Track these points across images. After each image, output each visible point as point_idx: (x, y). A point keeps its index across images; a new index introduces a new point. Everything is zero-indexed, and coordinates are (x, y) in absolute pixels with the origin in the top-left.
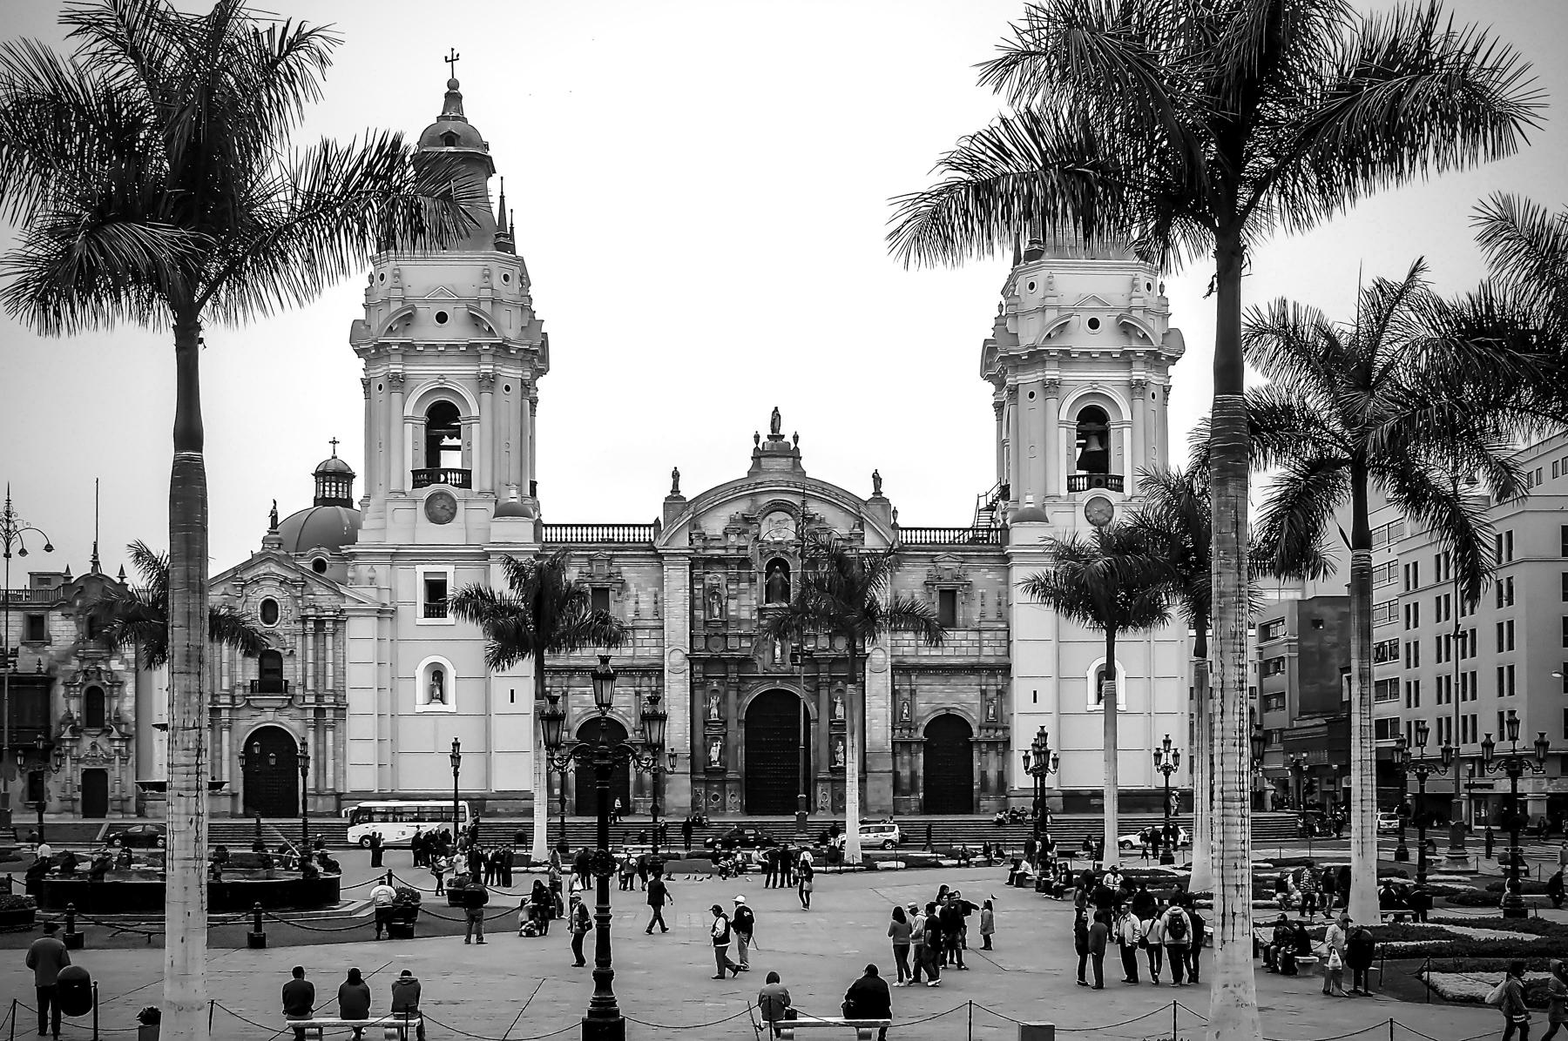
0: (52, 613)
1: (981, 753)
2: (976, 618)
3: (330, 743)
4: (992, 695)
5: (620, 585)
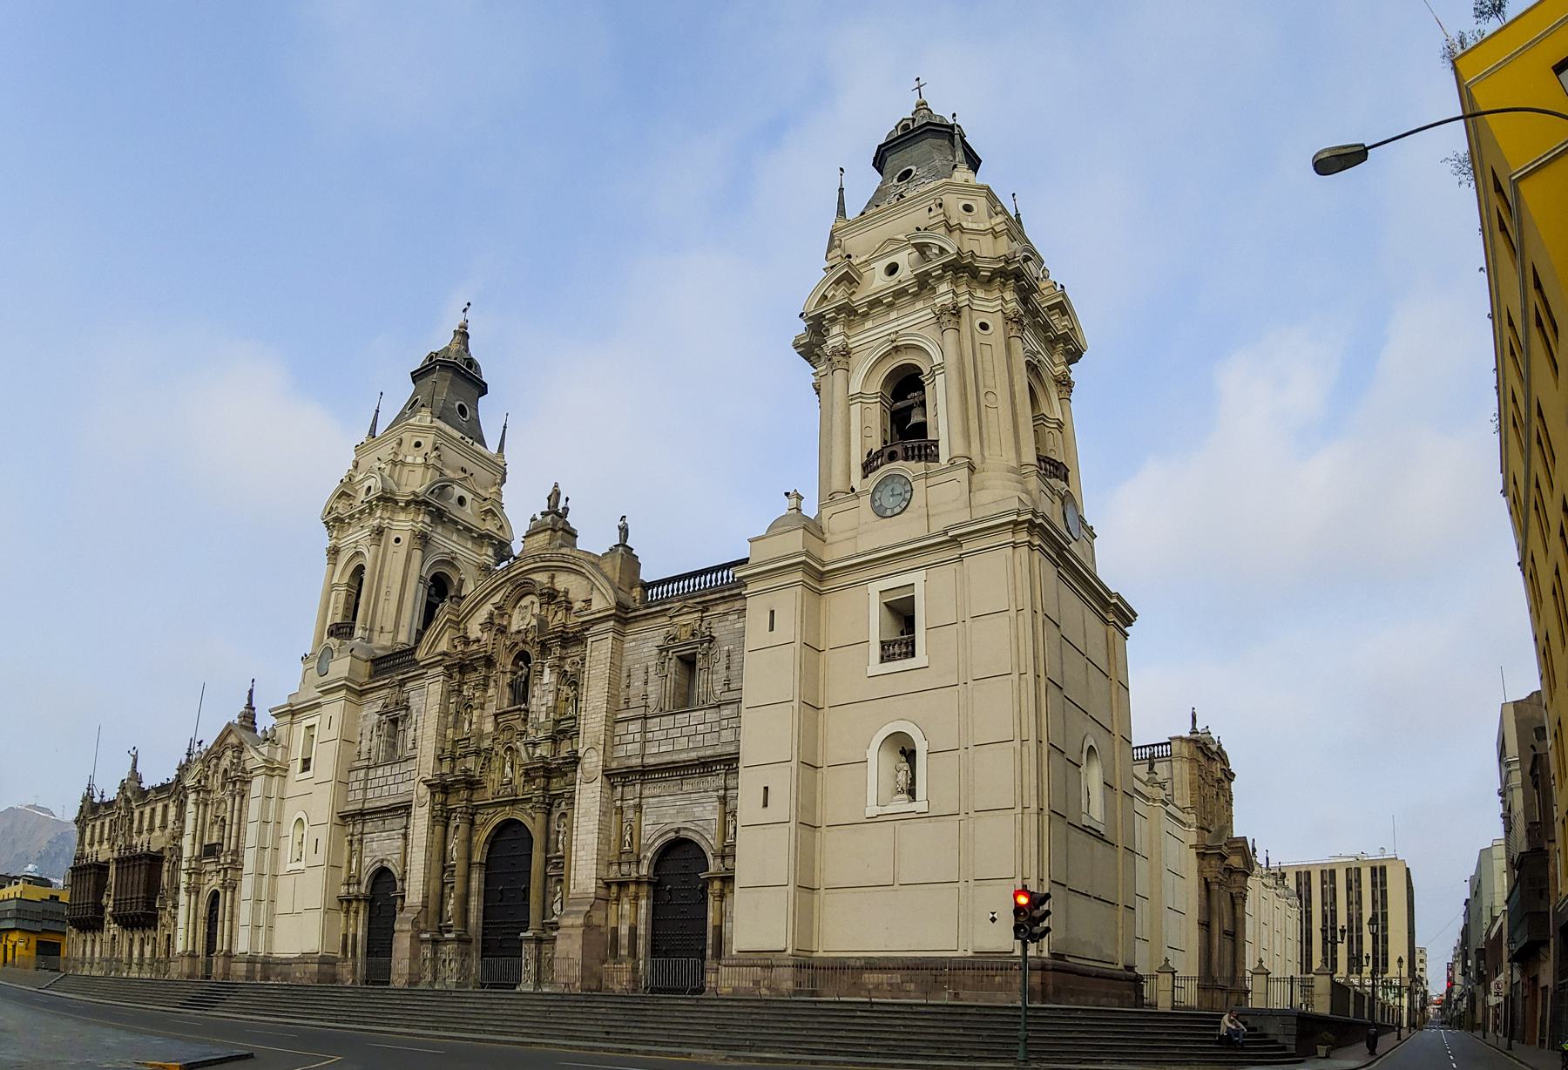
2: (718, 688)
5: (403, 712)
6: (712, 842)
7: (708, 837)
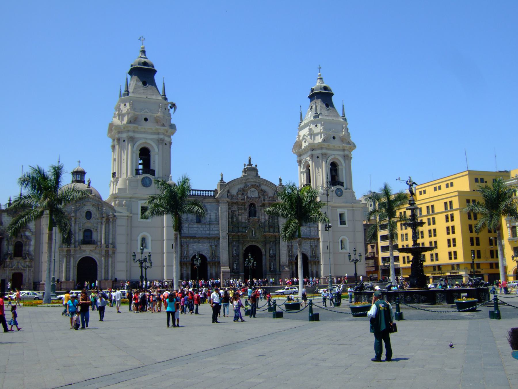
0: (3, 213)
3: (110, 262)
4: (314, 247)
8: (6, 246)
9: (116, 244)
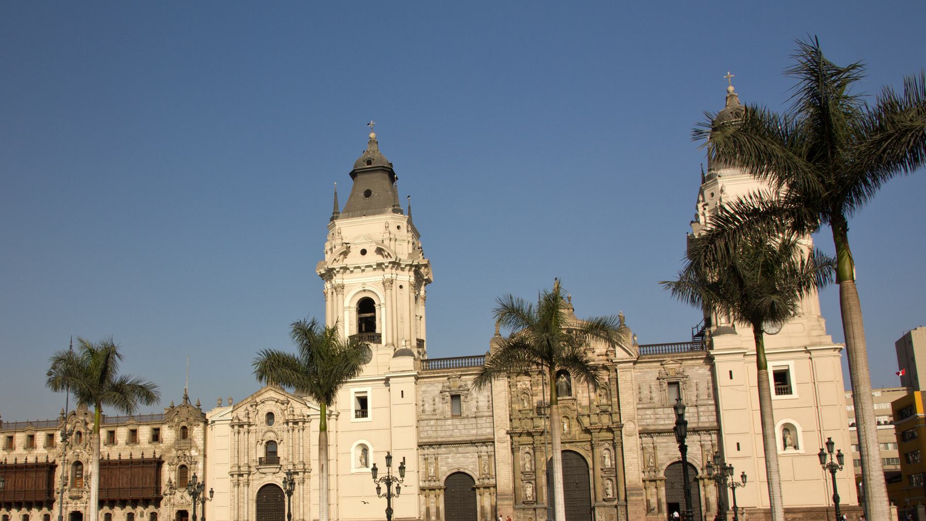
0: (163, 426)
1: (704, 486)
2: (694, 399)
5: (466, 392)
6: (698, 463)
7: (696, 461)
8: (168, 473)
9: (311, 461)
